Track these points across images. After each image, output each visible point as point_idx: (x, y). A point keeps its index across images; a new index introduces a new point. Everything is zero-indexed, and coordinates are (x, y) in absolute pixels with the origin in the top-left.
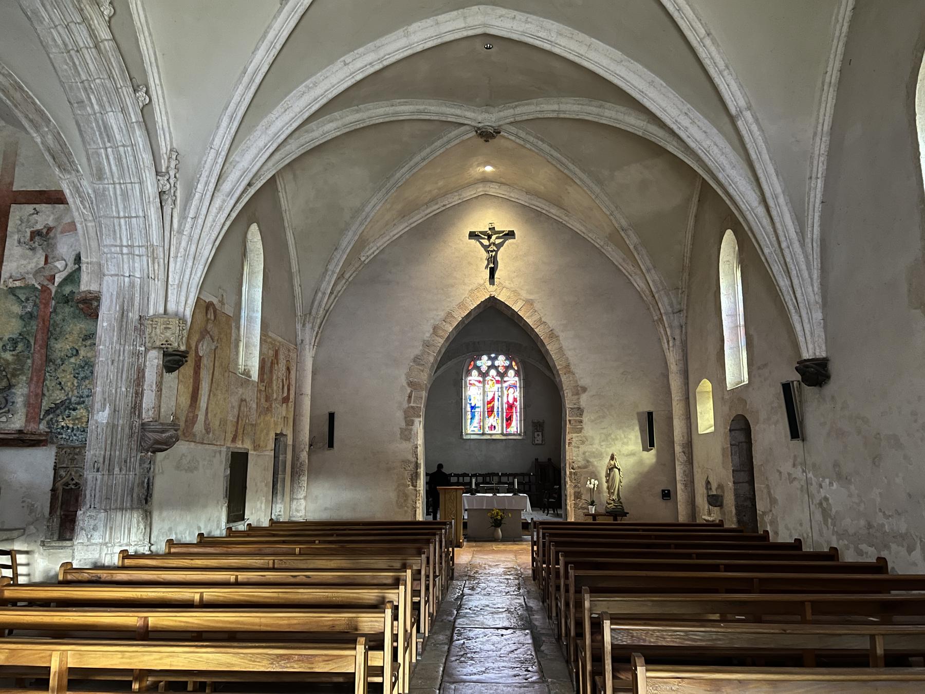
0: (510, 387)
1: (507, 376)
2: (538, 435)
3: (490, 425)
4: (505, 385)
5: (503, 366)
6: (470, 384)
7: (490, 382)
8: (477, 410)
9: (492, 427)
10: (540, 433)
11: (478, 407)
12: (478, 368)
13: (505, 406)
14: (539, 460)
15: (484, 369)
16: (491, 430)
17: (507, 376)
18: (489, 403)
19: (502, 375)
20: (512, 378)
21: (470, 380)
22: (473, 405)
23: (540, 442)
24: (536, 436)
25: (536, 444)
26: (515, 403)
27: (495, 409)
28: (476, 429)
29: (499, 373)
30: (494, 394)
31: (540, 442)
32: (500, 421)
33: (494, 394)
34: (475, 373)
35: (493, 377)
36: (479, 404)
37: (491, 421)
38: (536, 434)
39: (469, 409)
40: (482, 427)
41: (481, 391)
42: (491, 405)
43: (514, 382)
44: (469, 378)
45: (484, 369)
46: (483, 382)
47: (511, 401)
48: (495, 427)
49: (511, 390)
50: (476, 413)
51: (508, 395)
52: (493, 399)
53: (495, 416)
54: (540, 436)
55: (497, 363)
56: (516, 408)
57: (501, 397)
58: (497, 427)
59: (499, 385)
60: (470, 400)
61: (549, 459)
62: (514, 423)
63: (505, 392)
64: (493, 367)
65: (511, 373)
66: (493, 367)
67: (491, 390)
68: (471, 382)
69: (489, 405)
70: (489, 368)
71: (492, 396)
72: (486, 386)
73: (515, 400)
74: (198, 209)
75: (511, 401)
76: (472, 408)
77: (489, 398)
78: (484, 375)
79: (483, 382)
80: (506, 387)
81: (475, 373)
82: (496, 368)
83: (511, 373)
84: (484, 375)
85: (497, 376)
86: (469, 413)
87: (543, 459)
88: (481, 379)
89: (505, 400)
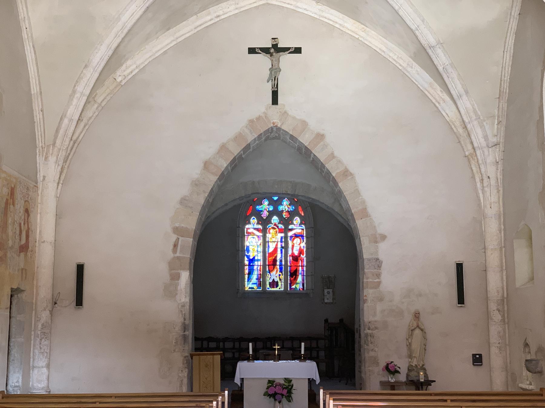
0: (296, 236)
1: (292, 223)
2: (328, 293)
3: (271, 281)
4: (290, 234)
5: (288, 211)
6: (249, 234)
7: (272, 231)
8: (256, 263)
9: (274, 284)
10: (331, 290)
11: (258, 260)
12: (258, 214)
13: (289, 259)
14: (329, 321)
15: (265, 214)
17: (292, 223)
18: (271, 254)
19: (286, 222)
20: (297, 226)
22: (251, 258)
23: (330, 300)
25: (326, 303)
26: (301, 255)
27: (278, 263)
28: (255, 287)
29: (282, 220)
30: (277, 245)
32: (282, 277)
33: (277, 245)
34: (254, 220)
35: (275, 225)
36: (260, 257)
37: (275, 275)
38: (326, 291)
39: (247, 262)
40: (261, 282)
41: (261, 241)
42: (273, 257)
43: (300, 231)
44: (247, 226)
45: (265, 214)
46: (264, 231)
47: (296, 253)
48: (277, 286)
49: (297, 241)
50: (255, 267)
51: (293, 246)
52: (276, 249)
53: (277, 271)
54: (331, 294)
55: (280, 208)
56: (302, 261)
57: (285, 248)
58: (280, 284)
59: (283, 235)
60: (248, 251)
61: (341, 320)
62: (300, 279)
64: (275, 212)
65: (297, 220)
66: (275, 212)
67: (274, 240)
68: (249, 231)
69: (271, 258)
70: (271, 214)
71: (274, 244)
72: (268, 235)
73: (301, 252)
74: (40, 127)
75: (296, 253)
76: (252, 261)
77: (271, 250)
78: (265, 222)
79: (264, 231)
80: (291, 237)
81: (254, 220)
82: (279, 214)
83: (297, 220)
84: (265, 222)
85: (279, 223)
86: (247, 267)
87: (334, 319)
88: (260, 227)
89: (290, 252)
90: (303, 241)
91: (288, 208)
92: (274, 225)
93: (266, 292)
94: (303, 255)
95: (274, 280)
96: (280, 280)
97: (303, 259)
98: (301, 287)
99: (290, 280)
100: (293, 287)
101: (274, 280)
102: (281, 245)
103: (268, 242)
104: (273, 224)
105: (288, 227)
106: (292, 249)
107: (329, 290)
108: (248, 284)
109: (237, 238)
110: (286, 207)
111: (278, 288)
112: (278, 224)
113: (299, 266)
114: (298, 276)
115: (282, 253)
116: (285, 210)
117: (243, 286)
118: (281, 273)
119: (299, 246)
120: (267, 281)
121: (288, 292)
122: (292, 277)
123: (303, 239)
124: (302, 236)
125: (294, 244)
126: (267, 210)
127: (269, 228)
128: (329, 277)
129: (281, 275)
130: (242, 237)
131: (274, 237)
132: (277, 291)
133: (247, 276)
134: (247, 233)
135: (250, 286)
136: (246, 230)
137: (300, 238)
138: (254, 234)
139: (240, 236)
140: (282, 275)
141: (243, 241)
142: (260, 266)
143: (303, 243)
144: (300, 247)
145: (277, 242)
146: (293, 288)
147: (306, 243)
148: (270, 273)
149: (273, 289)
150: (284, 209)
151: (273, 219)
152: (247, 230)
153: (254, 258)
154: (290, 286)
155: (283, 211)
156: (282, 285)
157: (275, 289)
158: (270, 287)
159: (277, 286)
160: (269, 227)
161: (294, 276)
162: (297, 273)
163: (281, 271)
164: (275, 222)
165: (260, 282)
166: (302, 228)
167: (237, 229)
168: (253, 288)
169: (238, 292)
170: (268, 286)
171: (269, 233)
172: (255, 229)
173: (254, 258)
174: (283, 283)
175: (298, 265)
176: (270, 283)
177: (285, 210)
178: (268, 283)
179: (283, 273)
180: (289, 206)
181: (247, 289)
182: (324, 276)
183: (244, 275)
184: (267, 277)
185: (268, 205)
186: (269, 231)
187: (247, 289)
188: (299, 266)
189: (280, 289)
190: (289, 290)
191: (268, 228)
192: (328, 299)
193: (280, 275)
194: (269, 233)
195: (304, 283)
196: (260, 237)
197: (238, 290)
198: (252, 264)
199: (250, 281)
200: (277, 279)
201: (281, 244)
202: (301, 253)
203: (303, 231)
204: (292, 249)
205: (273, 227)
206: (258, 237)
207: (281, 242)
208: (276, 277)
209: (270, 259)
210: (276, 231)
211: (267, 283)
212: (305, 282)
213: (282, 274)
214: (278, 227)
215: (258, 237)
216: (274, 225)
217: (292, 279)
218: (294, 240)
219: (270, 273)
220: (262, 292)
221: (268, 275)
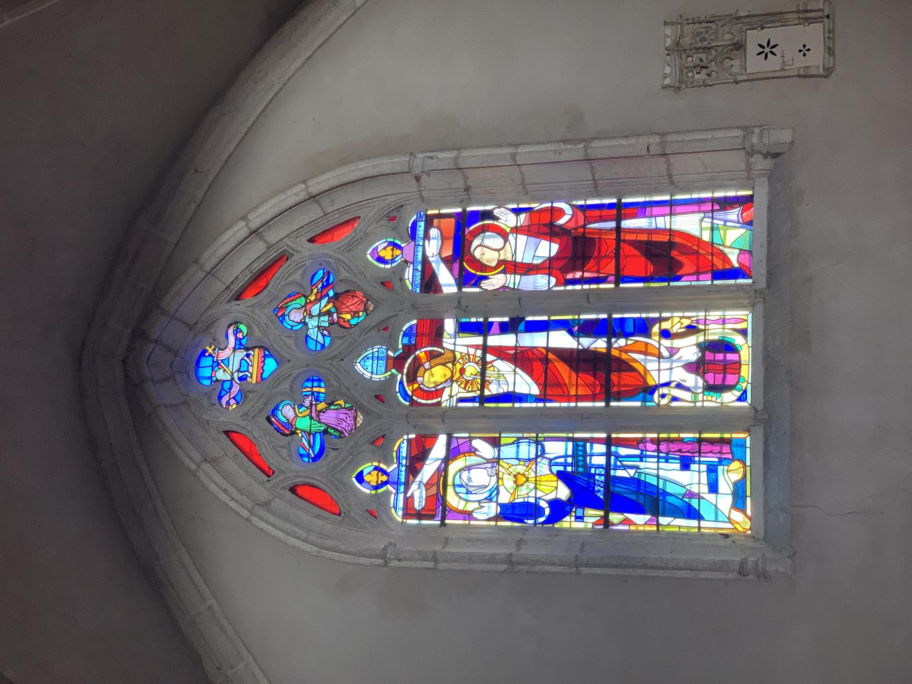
2: (768, 49)
10: (754, 38)
16: (737, 365)
21: (409, 511)
22: (564, 493)
24: (773, 64)
28: (729, 475)
30: (501, 353)
31: (814, 34)
32: (676, 321)
33: (501, 353)
39: (592, 516)
42: (563, 370)
47: (547, 249)
58: (715, 333)
59: (450, 325)
63: (496, 281)
67: (472, 370)
68: (419, 501)
71: (504, 366)
77: (525, 384)
90: (488, 215)
91: (318, 300)
92: (400, 370)
93: (760, 408)
94: (561, 212)
95: (690, 367)
96: (691, 329)
99: (698, 273)
101: (690, 367)
102: (504, 328)
104: (393, 376)
106: (528, 269)
107: (752, 49)
109: (441, 566)
110: (315, 309)
111: (738, 340)
112: (395, 350)
114: (671, 232)
116: (329, 313)
117: (723, 542)
118: (656, 329)
119: (511, 237)
120: (699, 404)
121: (763, 284)
122: (680, 265)
123: (476, 216)
124: (465, 220)
125: (500, 262)
127: (410, 393)
128: (677, 49)
130: (447, 541)
131: (459, 366)
132: (753, 347)
133: (663, 520)
134: (432, 517)
135: (725, 501)
137: (476, 233)
138: (442, 472)
139: (438, 548)
140: (666, 319)
141: (473, 536)
142: (608, 442)
143: (497, 219)
144: (516, 230)
145: (485, 349)
146: (739, 262)
148: (652, 390)
149: (746, 372)
150: (326, 318)
152: (419, 515)
155: (332, 323)
157: (745, 354)
158: (731, 388)
159: (728, 347)
160: (405, 395)
162: (655, 238)
163: (643, 327)
165: (705, 447)
167: (395, 563)
169: (763, 575)
170: (729, 398)
171: (438, 393)
172: (413, 470)
174: (714, 315)
176: (710, 388)
178: (712, 401)
179: (656, 315)
180: (313, 298)
181: (741, 521)
182: (667, 81)
183: (658, 537)
184: (674, 404)
186: (429, 394)
187: (741, 521)
188: (618, 228)
189: (744, 332)
190: (749, 281)
191: (413, 402)
192: (805, 50)
193: (665, 334)
195: (713, 201)
196: (454, 444)
197: (742, 571)
199: (694, 503)
200: (689, 350)
201: (495, 328)
202: (551, 225)
203: (436, 221)
204: (528, 269)
205: (407, 375)
206: (453, 453)
207: (482, 329)
210: (431, 356)
211: (706, 404)
212: (708, 195)
213: (660, 320)
215: (453, 453)
216: (400, 371)
217: (688, 267)
219: (652, 390)
220: (759, 431)
221: (663, 396)
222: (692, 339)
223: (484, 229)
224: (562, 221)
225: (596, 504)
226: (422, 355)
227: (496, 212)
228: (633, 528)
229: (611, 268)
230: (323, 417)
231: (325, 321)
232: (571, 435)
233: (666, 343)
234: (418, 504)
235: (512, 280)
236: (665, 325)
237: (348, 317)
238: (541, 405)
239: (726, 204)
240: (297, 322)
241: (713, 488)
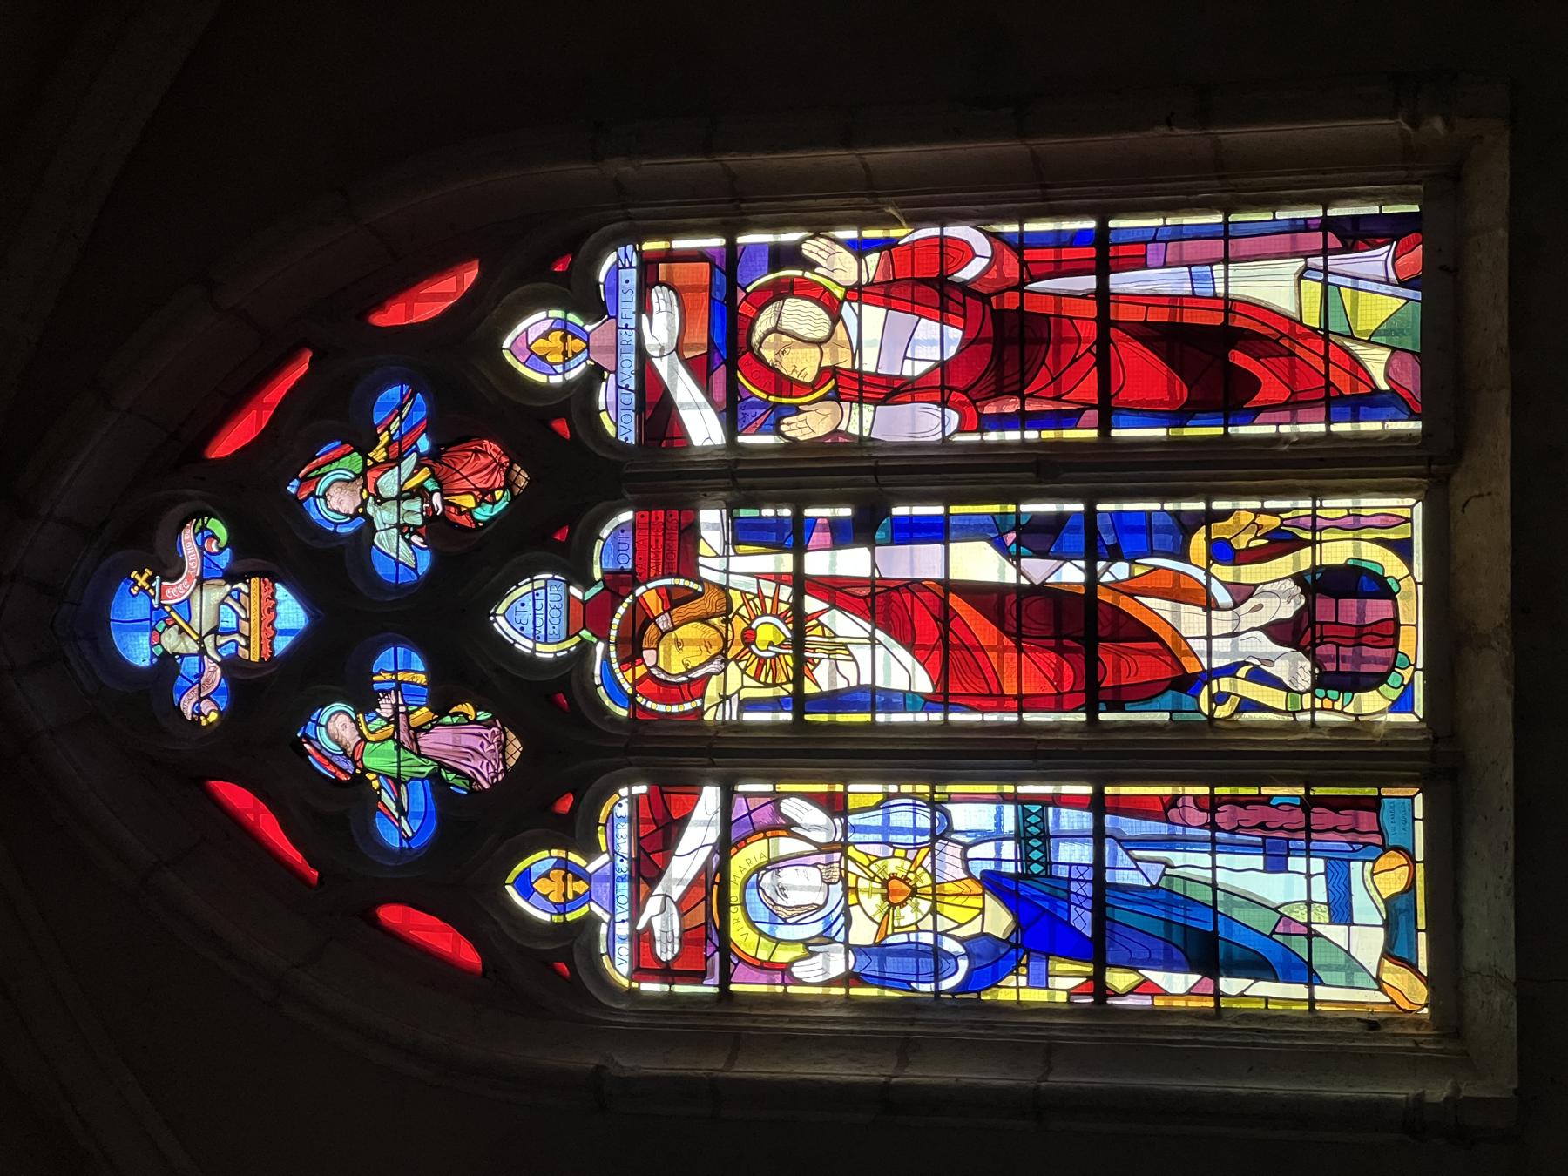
3: (1294, 667)
16: (1390, 630)
21: (644, 966)
22: (999, 921)
33: (837, 591)
42: (983, 631)
44: (620, 968)
53: (1179, 592)
58: (1336, 552)
67: (769, 632)
71: (845, 625)
80: (732, 412)
86: (1119, 979)
91: (394, 461)
94: (966, 252)
95: (1277, 631)
96: (1281, 542)
97: (1019, 245)
98: (1375, 261)
99: (1293, 406)
100: (1376, 362)
101: (1277, 631)
102: (842, 535)
103: (799, 702)
104: (585, 649)
105: (614, 445)
106: (892, 390)
108: (1351, 965)
110: (389, 483)
111: (1392, 566)
113: (1103, 295)
114: (1229, 304)
115: (936, 532)
116: (420, 492)
118: (1198, 543)
119: (847, 311)
122: (1254, 385)
126: (422, 715)
129: (1219, 530)
131: (739, 625)
133: (1230, 985)
134: (698, 977)
135: (1367, 943)
136: (652, 987)
138: (713, 880)
142: (1098, 805)
143: (811, 265)
144: (858, 293)
145: (801, 583)
146: (1387, 377)
147: (818, 228)
148: (1189, 683)
150: (415, 505)
151: (524, 645)
152: (667, 973)
153: (993, 883)
154: (1367, 402)
155: (431, 518)
156: (1354, 524)
158: (1375, 681)
159: (1373, 585)
161: (1239, 358)
162: (1190, 318)
164: (557, 627)
166: (630, 277)
168: (1396, 914)
170: (1371, 702)
171: (695, 687)
173: (993, 883)
174: (1335, 507)
175: (1091, 309)
176: (1324, 681)
177: (420, 492)
178: (1335, 711)
180: (379, 454)
185: (365, 702)
188: (1103, 295)
189: (1402, 549)
193: (1221, 552)
194: (695, 687)
195: (1327, 224)
198: (1082, 921)
199: (1299, 946)
201: (818, 537)
204: (892, 390)
207: (795, 538)
208: (1242, 593)
209: (1010, 688)
210: (673, 599)
213: (1211, 517)
214: (619, 585)
217: (1272, 389)
218: (781, 383)
219: (1189, 683)
221: (1218, 699)
222: (1284, 565)
223: (781, 291)
224: (969, 272)
225: (1073, 947)
226: (653, 602)
227: (810, 249)
228: (1159, 1002)
229: (1088, 389)
230: (427, 742)
231: (414, 511)
232: (1009, 789)
233: (1223, 572)
234: (666, 951)
235: (861, 421)
236: (1219, 530)
237: (468, 501)
238: (936, 717)
239: (1355, 236)
240: (347, 515)
241: (1341, 912)
